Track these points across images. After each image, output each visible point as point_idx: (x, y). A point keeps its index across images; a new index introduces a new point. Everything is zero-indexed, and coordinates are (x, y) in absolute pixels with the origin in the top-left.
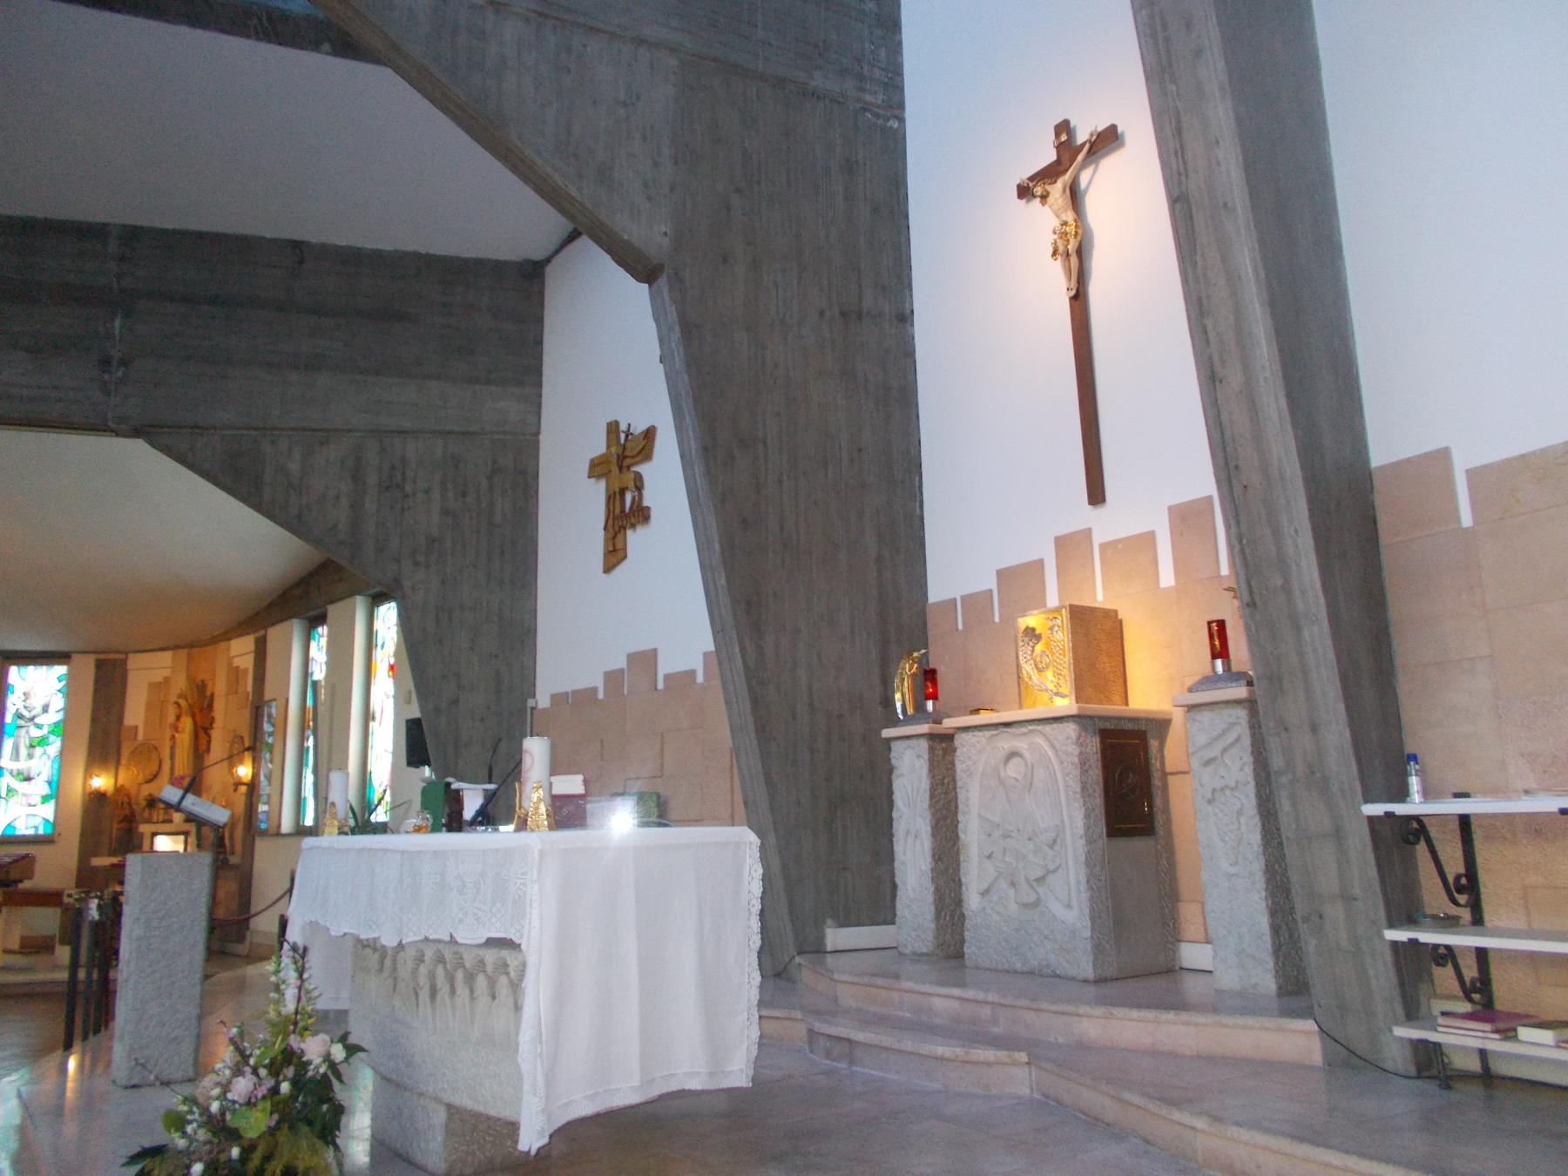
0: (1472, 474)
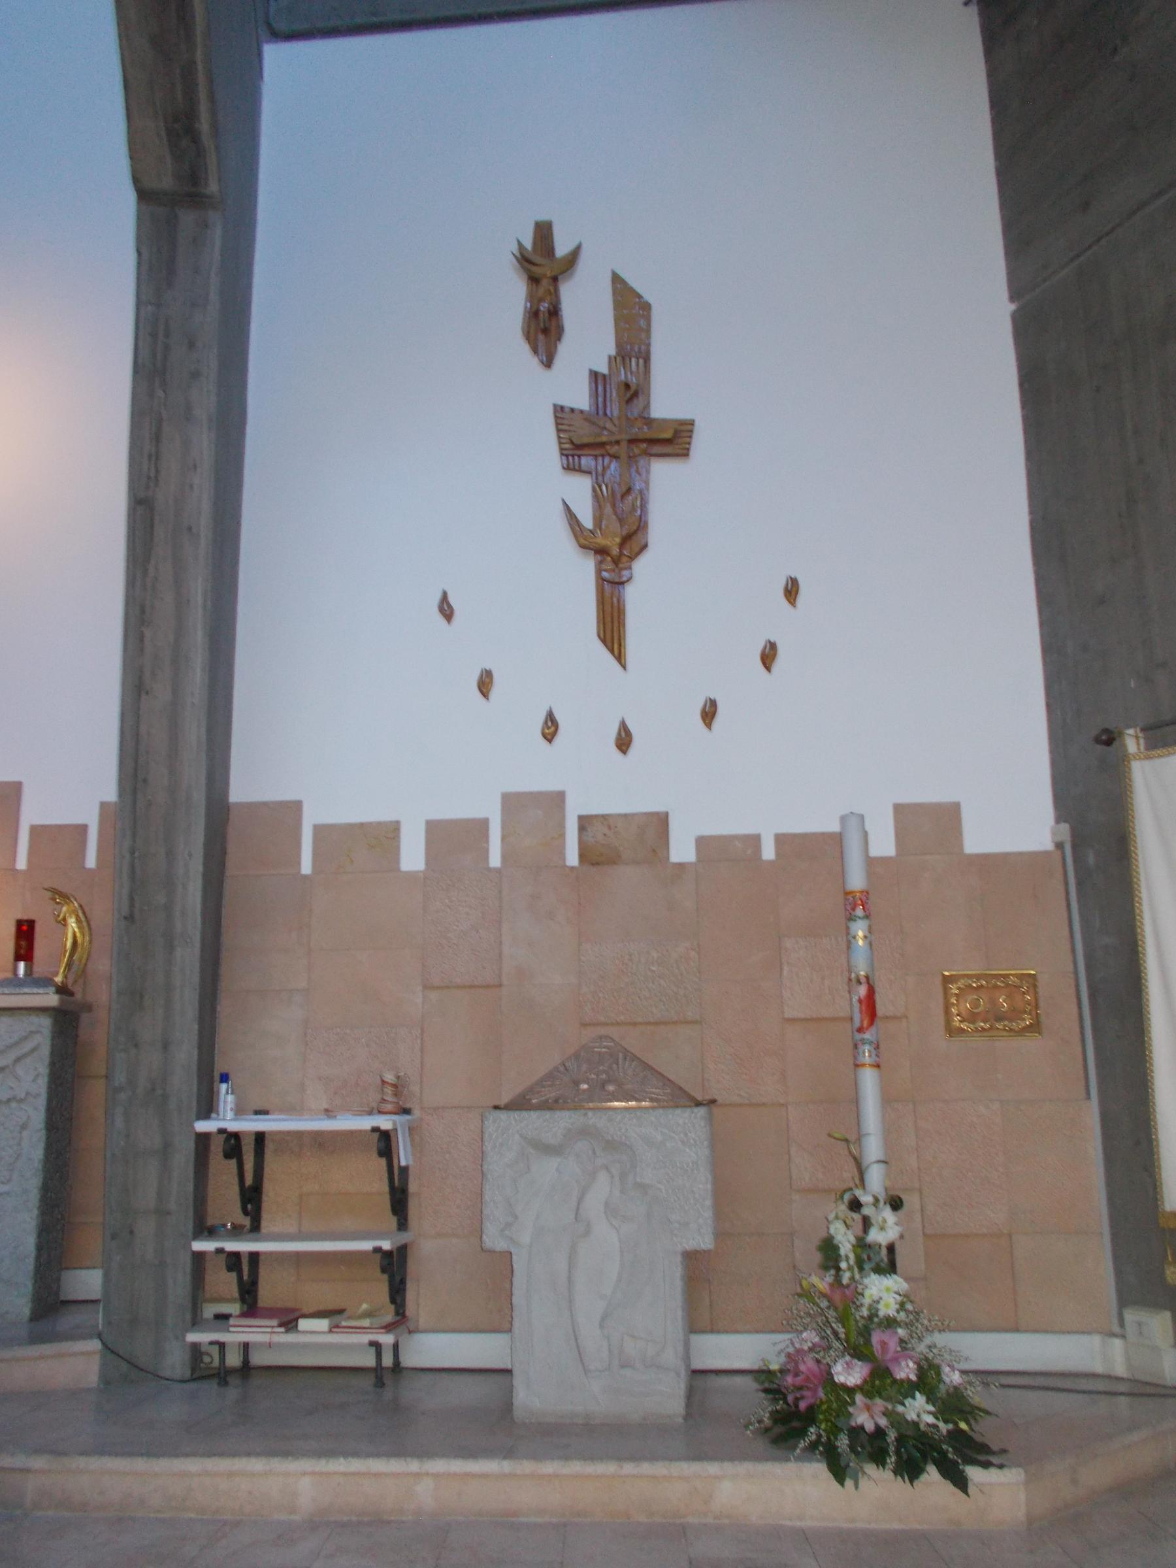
0: (318, 829)
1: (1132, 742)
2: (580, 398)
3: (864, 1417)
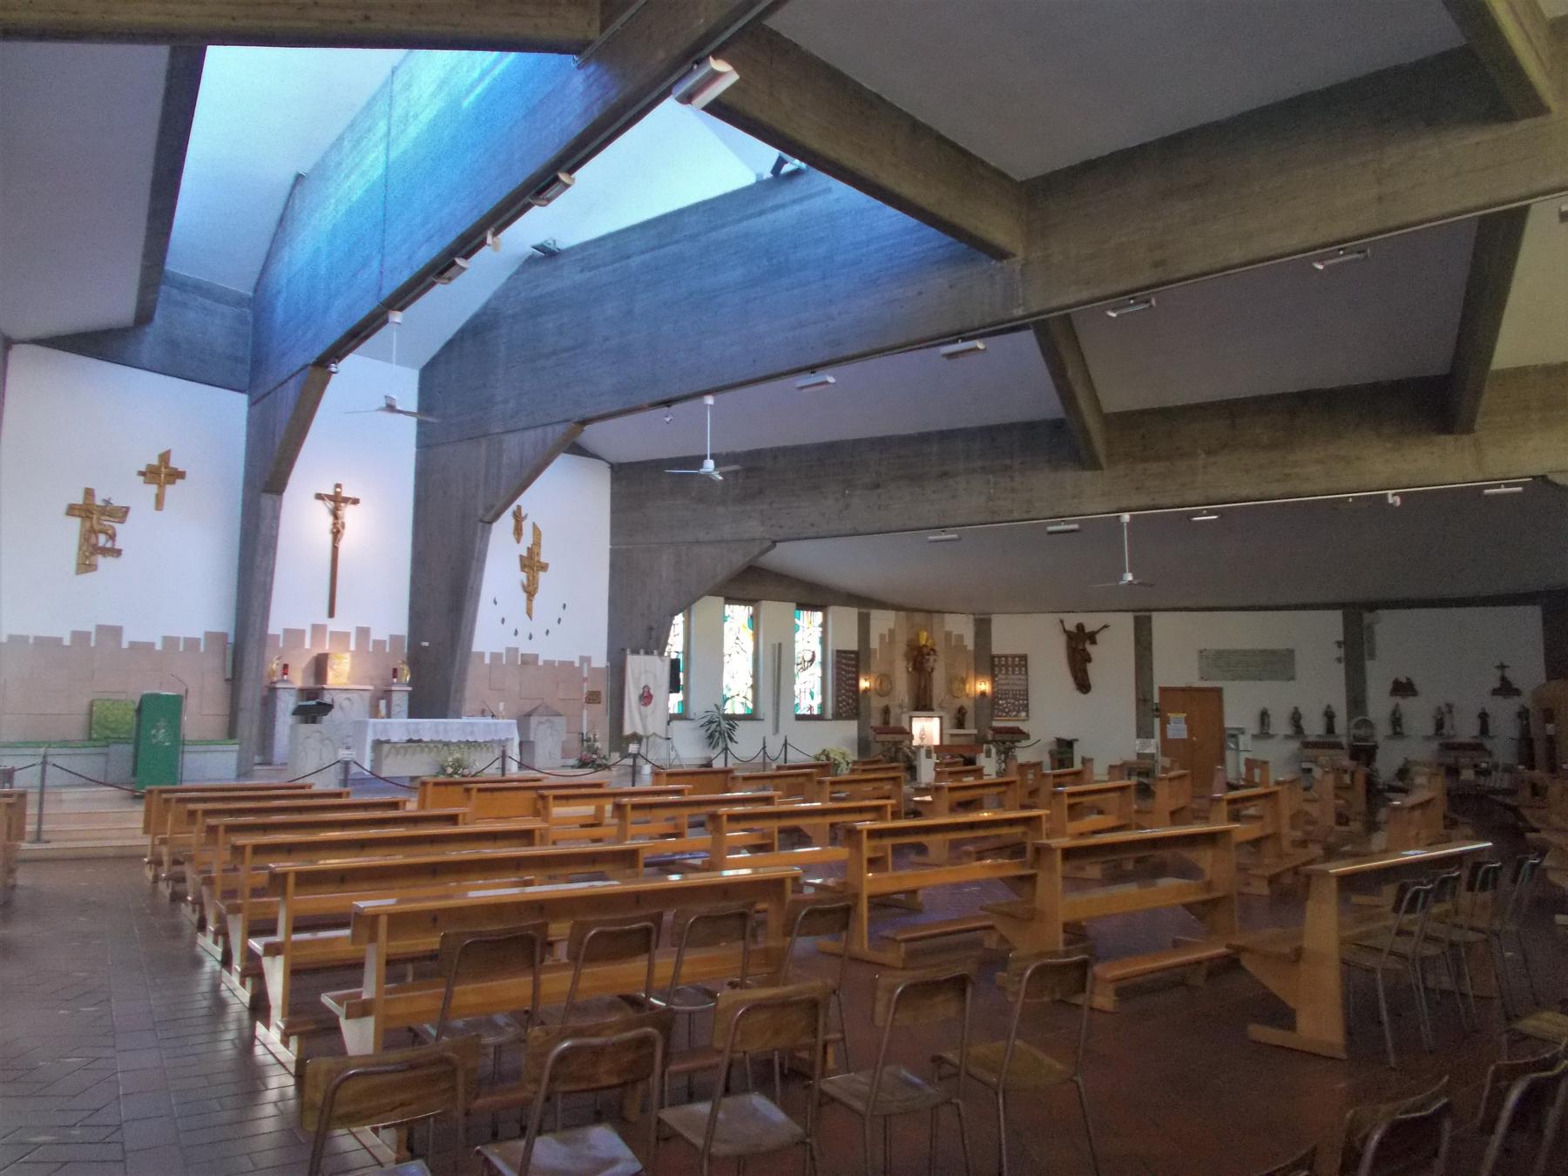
1: (628, 652)
2: (525, 554)
3: (599, 762)
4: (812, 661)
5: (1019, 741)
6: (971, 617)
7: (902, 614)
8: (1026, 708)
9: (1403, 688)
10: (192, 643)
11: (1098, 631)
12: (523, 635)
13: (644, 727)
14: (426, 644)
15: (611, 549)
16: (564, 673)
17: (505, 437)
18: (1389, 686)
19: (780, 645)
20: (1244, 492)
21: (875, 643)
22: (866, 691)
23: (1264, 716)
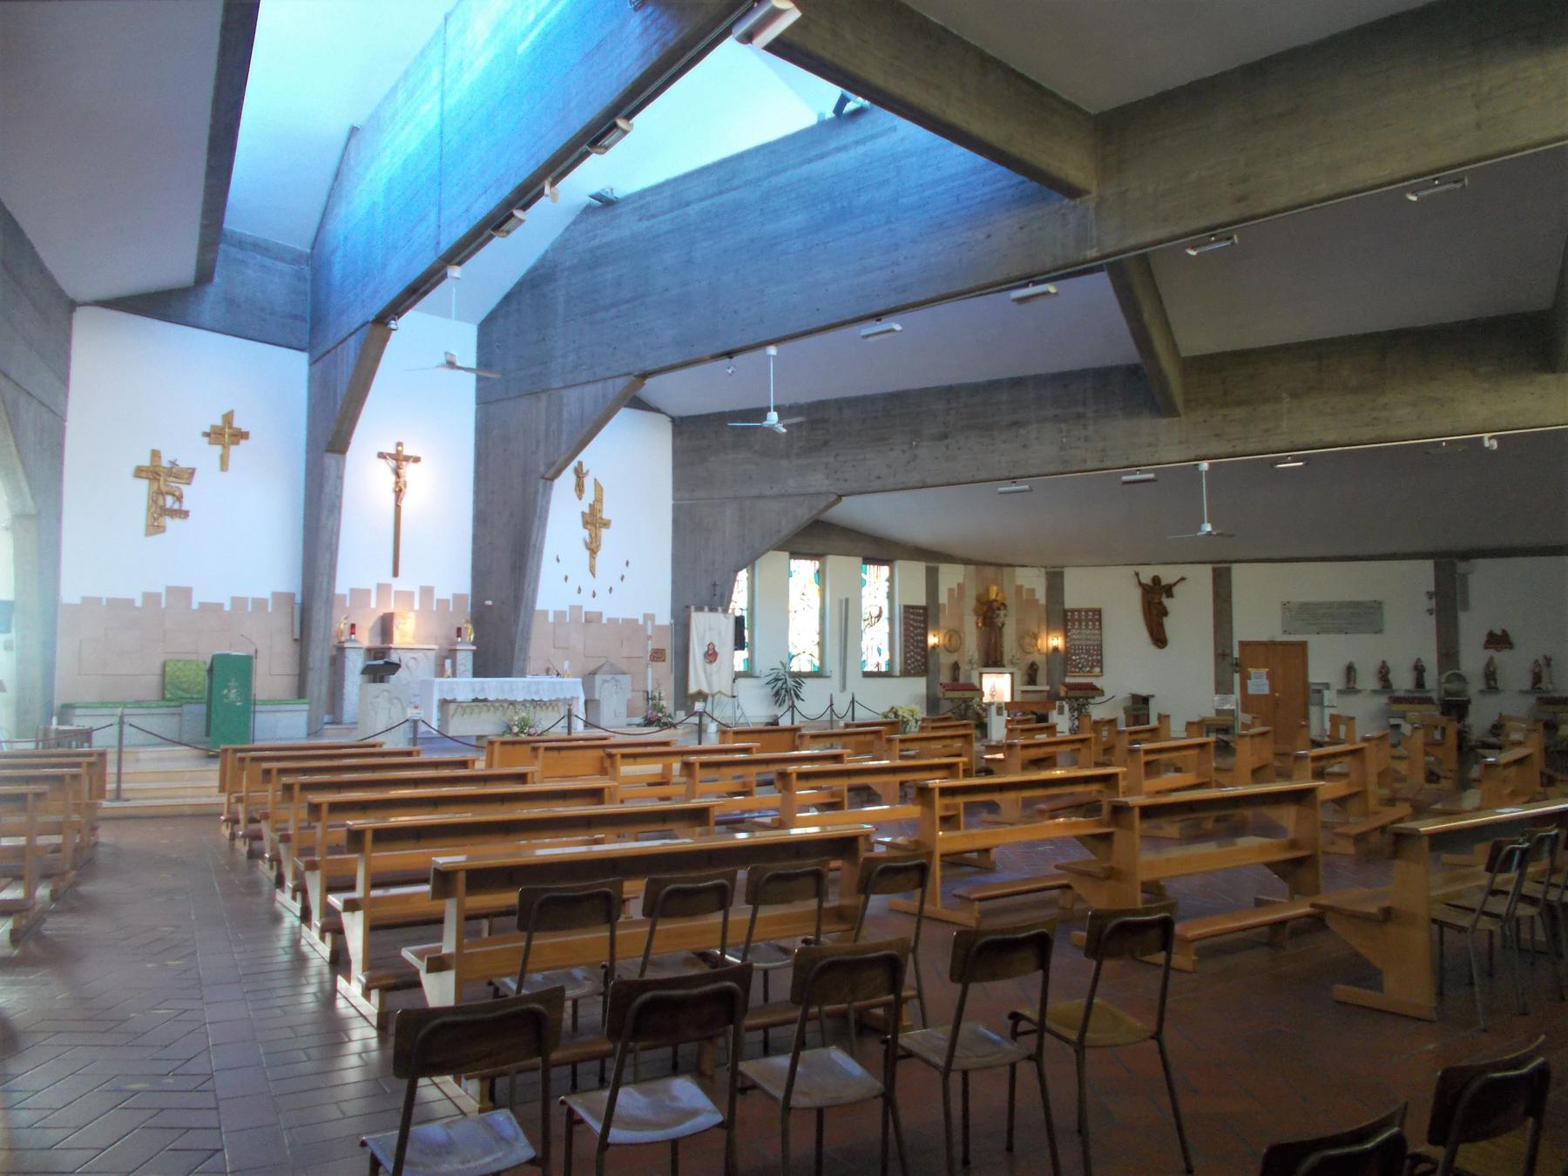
1: (693, 608)
2: (587, 510)
3: (664, 720)
4: (879, 616)
5: (1093, 698)
6: (1043, 570)
7: (971, 568)
8: (1100, 663)
9: (1498, 641)
10: (260, 604)
11: (1175, 584)
12: (587, 593)
13: (710, 684)
14: (489, 603)
15: (673, 505)
16: (630, 628)
17: (564, 392)
18: (1483, 638)
19: (847, 600)
20: (1330, 438)
21: (943, 598)
22: (934, 647)
23: (1350, 670)
